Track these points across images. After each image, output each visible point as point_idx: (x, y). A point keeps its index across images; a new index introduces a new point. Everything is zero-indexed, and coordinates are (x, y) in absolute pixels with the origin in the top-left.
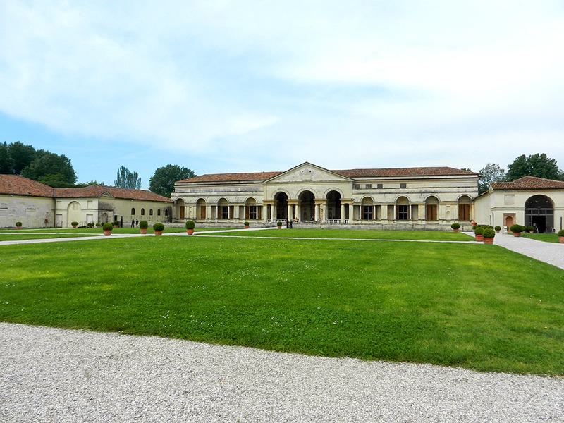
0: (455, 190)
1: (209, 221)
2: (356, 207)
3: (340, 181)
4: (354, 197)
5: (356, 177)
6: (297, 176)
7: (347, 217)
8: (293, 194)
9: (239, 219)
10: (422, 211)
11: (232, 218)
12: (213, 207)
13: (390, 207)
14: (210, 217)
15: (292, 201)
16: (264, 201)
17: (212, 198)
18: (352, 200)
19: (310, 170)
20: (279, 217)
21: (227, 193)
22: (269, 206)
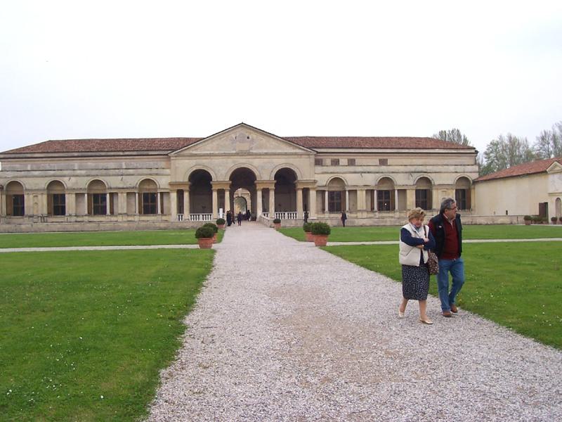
0: (452, 168)
1: (74, 219)
2: (321, 193)
3: (296, 154)
4: (317, 177)
5: (314, 146)
6: (226, 145)
7: (306, 208)
8: (221, 172)
9: (127, 214)
10: (411, 198)
11: (112, 213)
12: (79, 196)
13: (370, 192)
16: (171, 184)
18: (315, 182)
19: (247, 135)
20: (193, 210)
21: (104, 172)
22: (180, 194)
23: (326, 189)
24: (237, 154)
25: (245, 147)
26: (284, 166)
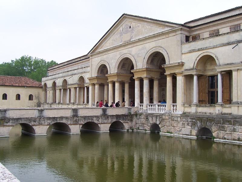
2: (189, 78)
3: (163, 34)
12: (61, 89)
16: (90, 79)
17: (59, 82)
18: (182, 64)
23: (193, 73)
24: (120, 46)
25: (126, 38)
26: (155, 50)
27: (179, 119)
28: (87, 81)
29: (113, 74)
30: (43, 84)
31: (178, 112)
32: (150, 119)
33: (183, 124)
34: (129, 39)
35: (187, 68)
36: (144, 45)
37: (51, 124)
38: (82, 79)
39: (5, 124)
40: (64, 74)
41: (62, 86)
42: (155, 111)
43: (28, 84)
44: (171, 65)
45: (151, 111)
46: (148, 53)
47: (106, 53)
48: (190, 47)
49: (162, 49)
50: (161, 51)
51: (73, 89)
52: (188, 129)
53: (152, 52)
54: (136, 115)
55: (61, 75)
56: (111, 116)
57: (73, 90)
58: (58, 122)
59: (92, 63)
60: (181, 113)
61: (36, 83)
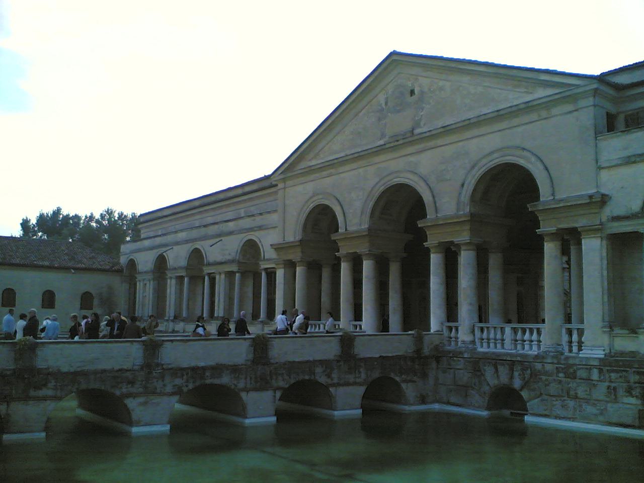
3: (529, 107)
12: (180, 279)
14: (172, 315)
15: (350, 237)
16: (278, 248)
17: (177, 257)
21: (203, 231)
24: (379, 150)
25: (400, 123)
26: (497, 160)
27: (595, 375)
28: (268, 253)
29: (356, 232)
30: (123, 260)
31: (590, 352)
32: (489, 372)
33: (612, 391)
34: (407, 126)
35: (621, 212)
36: (461, 144)
37: (185, 389)
38: (251, 248)
39: (32, 393)
40: (194, 234)
41: (187, 268)
42: (503, 347)
43: (81, 262)
44: (561, 205)
45: (489, 347)
46: (476, 168)
47: (332, 171)
48: (626, 149)
49: (525, 153)
50: (522, 162)
51: (223, 276)
52: (628, 406)
53: (492, 164)
54: (438, 359)
55: (182, 236)
56: (365, 360)
57: (221, 282)
58: (208, 381)
59: (287, 202)
60: (600, 354)
61: (102, 261)
